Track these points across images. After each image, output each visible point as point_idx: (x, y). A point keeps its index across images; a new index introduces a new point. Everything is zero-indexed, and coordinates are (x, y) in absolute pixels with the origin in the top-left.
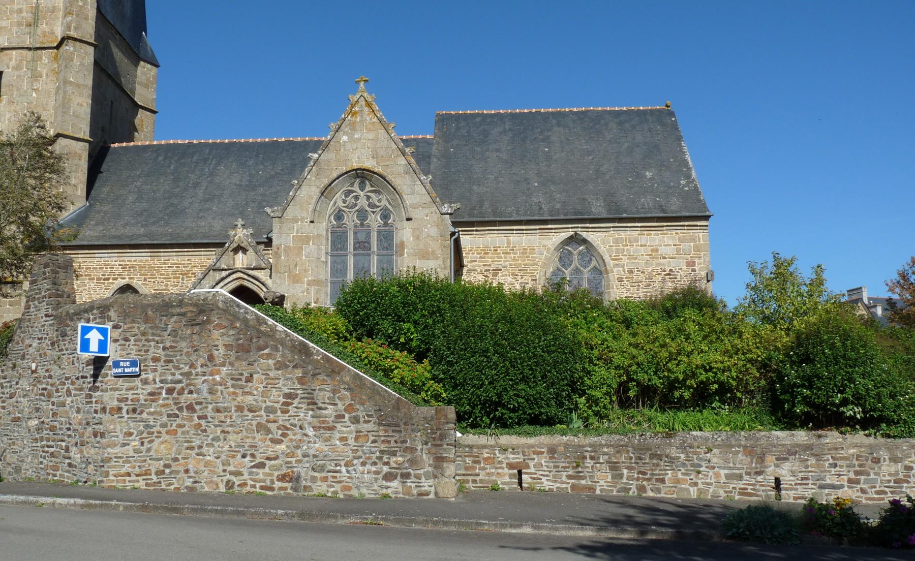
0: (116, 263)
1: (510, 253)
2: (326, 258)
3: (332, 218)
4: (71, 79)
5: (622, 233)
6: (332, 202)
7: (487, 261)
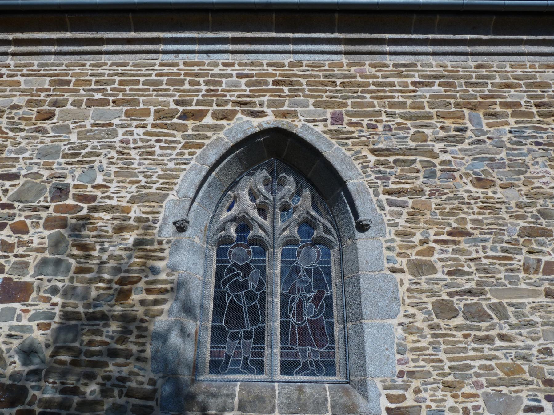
0: (229, 70)
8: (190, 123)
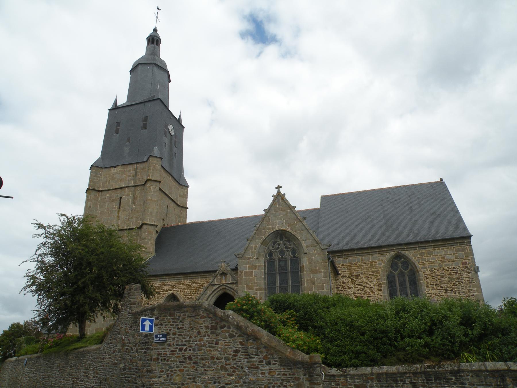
0: (167, 283)
1: (364, 266)
2: (265, 276)
3: (267, 256)
4: (149, 198)
5: (424, 250)
6: (267, 248)
7: (352, 271)
8: (163, 293)
